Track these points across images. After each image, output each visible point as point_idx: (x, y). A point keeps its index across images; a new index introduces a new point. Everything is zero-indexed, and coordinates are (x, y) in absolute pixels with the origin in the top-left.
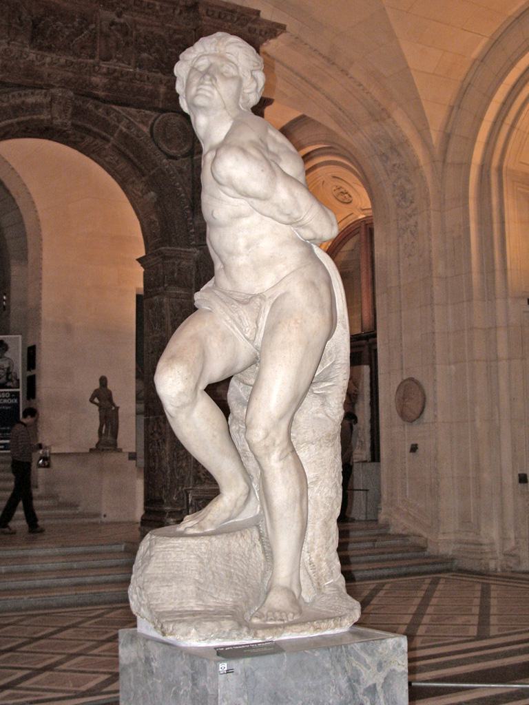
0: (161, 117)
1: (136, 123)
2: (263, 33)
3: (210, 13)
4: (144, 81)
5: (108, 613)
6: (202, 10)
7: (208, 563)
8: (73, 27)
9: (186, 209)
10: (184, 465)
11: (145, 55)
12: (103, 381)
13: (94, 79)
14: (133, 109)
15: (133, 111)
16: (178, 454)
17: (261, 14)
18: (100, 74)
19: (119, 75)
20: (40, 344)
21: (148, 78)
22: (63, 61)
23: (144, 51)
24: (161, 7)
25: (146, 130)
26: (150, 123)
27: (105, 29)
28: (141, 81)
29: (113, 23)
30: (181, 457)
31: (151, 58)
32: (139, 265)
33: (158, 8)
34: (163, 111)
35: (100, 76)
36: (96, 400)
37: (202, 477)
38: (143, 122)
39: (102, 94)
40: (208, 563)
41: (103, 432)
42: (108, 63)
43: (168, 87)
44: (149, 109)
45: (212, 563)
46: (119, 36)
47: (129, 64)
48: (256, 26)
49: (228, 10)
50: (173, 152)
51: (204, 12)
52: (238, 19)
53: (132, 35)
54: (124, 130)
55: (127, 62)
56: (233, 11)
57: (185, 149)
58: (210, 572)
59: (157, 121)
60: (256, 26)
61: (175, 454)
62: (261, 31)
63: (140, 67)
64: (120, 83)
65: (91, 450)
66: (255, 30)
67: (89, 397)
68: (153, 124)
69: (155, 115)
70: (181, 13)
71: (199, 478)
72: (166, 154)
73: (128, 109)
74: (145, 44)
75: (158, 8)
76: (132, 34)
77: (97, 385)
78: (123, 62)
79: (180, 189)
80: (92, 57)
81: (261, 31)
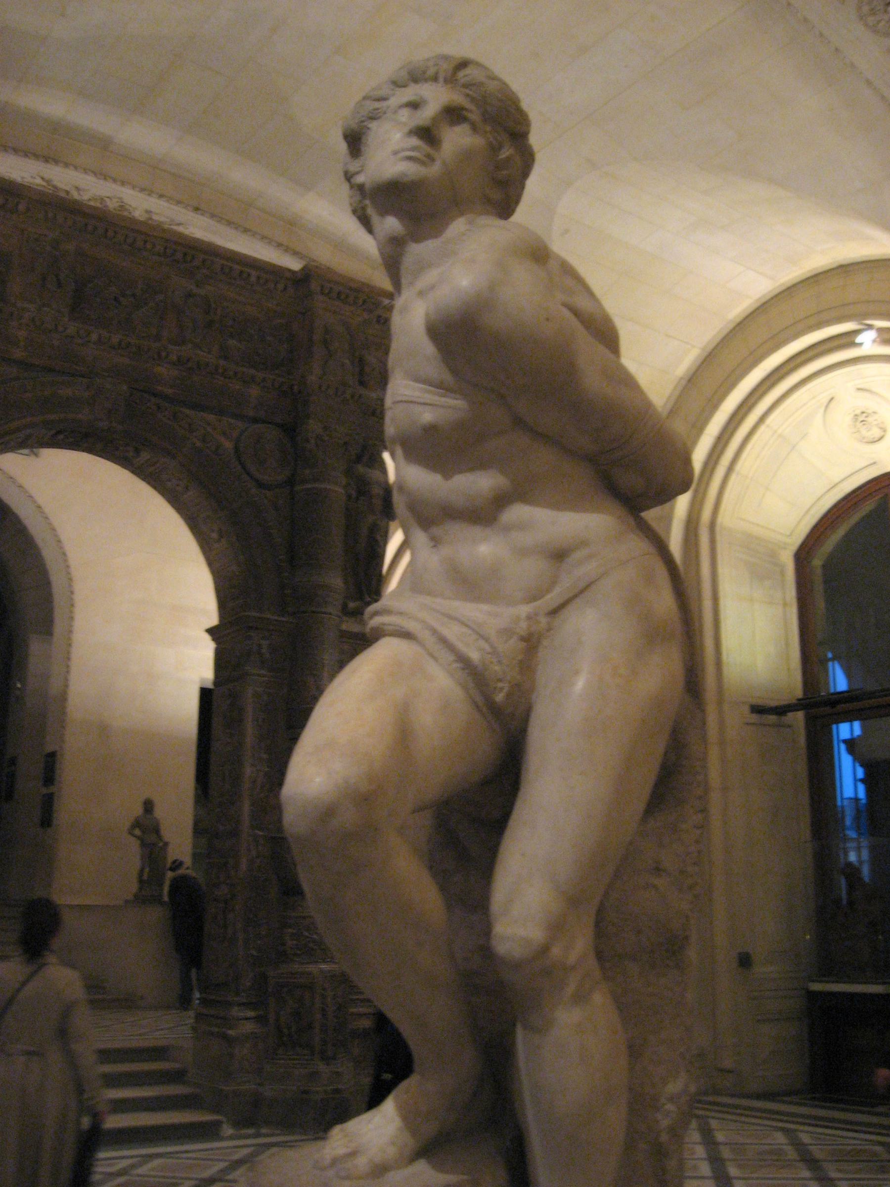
5: (140, 1165)
6: (314, 286)
8: (134, 295)
11: (232, 342)
12: (148, 806)
13: (159, 369)
15: (211, 418)
20: (61, 747)
21: (236, 373)
22: (115, 339)
23: (232, 336)
24: (258, 278)
25: (228, 445)
29: (189, 295)
32: (207, 638)
33: (253, 279)
34: (255, 420)
36: (137, 832)
39: (169, 391)
41: (145, 877)
44: (236, 416)
47: (209, 353)
49: (351, 289)
52: (364, 302)
54: (198, 444)
63: (226, 358)
65: (127, 901)
67: (128, 824)
70: (285, 289)
72: (257, 481)
73: (205, 415)
75: (253, 279)
77: (138, 810)
80: (158, 338)
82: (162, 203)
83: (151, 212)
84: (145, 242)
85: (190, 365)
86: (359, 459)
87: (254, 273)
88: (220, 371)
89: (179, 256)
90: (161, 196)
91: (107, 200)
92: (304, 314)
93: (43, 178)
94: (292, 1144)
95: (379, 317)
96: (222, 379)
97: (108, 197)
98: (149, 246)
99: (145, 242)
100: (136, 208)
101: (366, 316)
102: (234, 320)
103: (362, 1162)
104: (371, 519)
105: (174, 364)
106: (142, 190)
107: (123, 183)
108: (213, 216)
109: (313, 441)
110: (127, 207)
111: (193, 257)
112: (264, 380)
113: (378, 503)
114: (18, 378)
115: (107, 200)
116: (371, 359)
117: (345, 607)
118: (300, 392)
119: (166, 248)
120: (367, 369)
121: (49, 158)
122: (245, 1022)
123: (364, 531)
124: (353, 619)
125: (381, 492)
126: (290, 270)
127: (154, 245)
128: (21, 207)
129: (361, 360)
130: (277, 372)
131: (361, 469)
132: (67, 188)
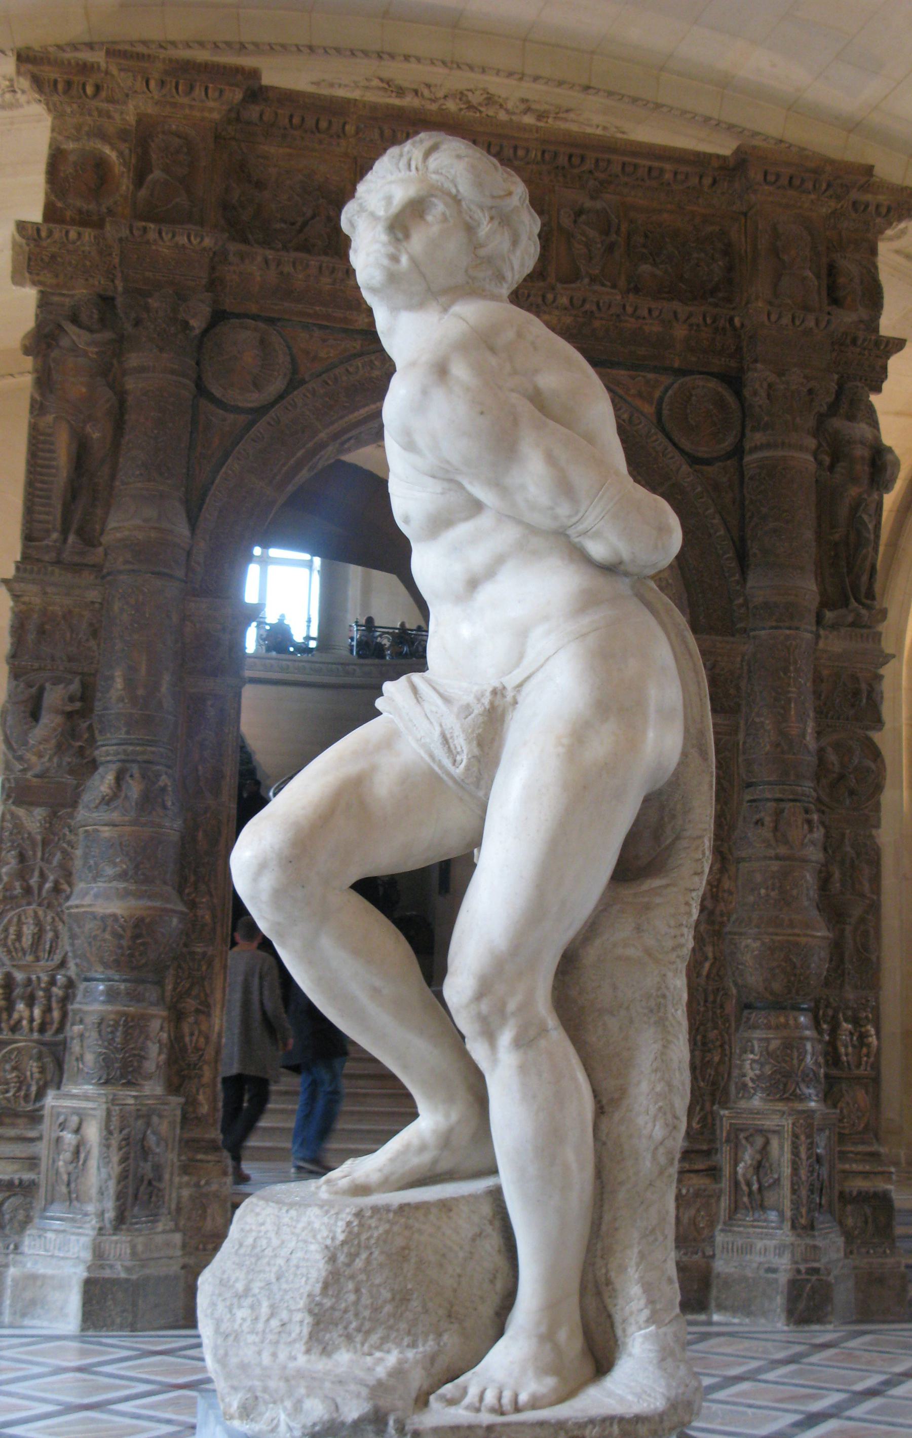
0: (676, 386)
1: (630, 399)
2: (884, 210)
3: (771, 178)
4: (644, 318)
6: (755, 174)
7: (349, 1265)
9: (727, 559)
10: (716, 1059)
11: (645, 268)
14: (622, 372)
16: (704, 1037)
17: (877, 171)
18: (557, 308)
19: (594, 308)
21: (650, 311)
24: (676, 174)
25: (649, 409)
26: (657, 394)
27: (566, 221)
28: (638, 318)
29: (579, 213)
30: (710, 1045)
31: (659, 273)
33: (668, 176)
34: (681, 372)
35: (556, 312)
37: (750, 1084)
38: (640, 395)
40: (349, 1265)
42: (573, 285)
43: (691, 325)
44: (655, 369)
45: (359, 1263)
46: (592, 233)
47: (614, 286)
48: (869, 197)
50: (703, 451)
51: (760, 177)
53: (618, 232)
55: (608, 284)
56: (817, 171)
57: (722, 446)
58: (351, 1286)
59: (670, 392)
60: (869, 197)
61: (699, 1037)
62: (878, 207)
64: (597, 324)
66: (867, 206)
68: (661, 400)
69: (666, 380)
71: (745, 1085)
74: (644, 246)
75: (668, 176)
76: (619, 229)
78: (603, 285)
79: (716, 521)
81: (878, 207)
82: (540, 87)
83: (527, 101)
84: (515, 148)
85: (587, 306)
86: (833, 409)
87: (668, 167)
88: (629, 310)
89: (562, 160)
90: (536, 79)
91: (470, 94)
92: (745, 214)
93: (381, 80)
94: (750, 1335)
95: (854, 203)
96: (633, 320)
97: (468, 90)
98: (521, 153)
99: (515, 148)
100: (507, 99)
101: (832, 203)
102: (646, 236)
103: (344, 1183)
104: (853, 491)
105: (566, 309)
106: (510, 75)
107: (483, 71)
108: (610, 94)
109: (763, 393)
110: (496, 98)
111: (583, 158)
112: (690, 315)
113: (862, 469)
114: (361, 355)
115: (470, 94)
116: (848, 265)
117: (819, 620)
118: (742, 325)
119: (543, 152)
120: (841, 280)
121: (383, 52)
122: (692, 1175)
123: (843, 511)
124: (835, 633)
125: (867, 453)
126: (718, 156)
127: (528, 151)
128: (350, 129)
129: (832, 270)
130: (711, 300)
131: (837, 423)
132: (415, 87)
